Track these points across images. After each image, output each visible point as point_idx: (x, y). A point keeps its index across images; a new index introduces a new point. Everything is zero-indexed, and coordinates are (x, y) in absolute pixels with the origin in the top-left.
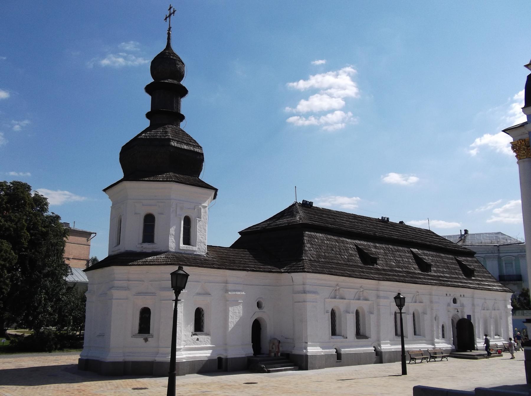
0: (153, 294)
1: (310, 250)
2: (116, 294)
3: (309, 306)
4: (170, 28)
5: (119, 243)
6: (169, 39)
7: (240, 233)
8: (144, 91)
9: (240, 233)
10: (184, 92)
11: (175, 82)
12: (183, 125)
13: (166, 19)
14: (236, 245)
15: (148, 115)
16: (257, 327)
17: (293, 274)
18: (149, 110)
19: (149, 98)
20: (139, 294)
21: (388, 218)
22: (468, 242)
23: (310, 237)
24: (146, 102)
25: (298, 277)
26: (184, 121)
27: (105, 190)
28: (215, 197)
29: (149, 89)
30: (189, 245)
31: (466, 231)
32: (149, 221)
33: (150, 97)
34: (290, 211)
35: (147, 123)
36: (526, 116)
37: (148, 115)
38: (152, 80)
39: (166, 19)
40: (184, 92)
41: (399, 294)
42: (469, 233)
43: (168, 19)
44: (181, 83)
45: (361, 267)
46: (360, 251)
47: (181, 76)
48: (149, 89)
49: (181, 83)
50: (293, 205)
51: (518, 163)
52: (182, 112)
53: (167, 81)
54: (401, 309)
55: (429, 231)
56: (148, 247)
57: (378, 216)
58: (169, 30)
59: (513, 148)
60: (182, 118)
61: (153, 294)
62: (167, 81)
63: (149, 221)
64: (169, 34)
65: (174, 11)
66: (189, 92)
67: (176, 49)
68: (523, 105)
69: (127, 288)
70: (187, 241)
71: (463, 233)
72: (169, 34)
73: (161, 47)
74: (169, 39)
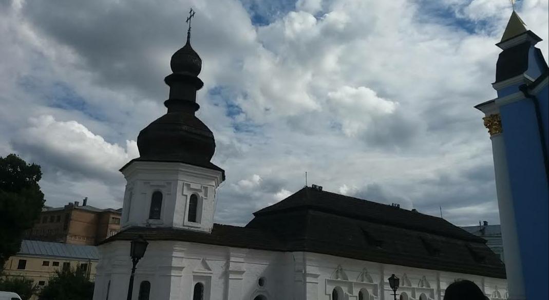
3: (308, 286)
4: (190, 28)
5: (128, 221)
6: (189, 37)
7: (254, 214)
8: (164, 82)
9: (254, 214)
12: (197, 114)
13: (187, 21)
14: (250, 225)
17: (294, 253)
18: (168, 98)
21: (398, 205)
22: (487, 233)
26: (199, 110)
27: (121, 170)
28: (224, 178)
29: (168, 80)
30: (194, 221)
31: (485, 223)
32: (157, 199)
33: (169, 88)
35: (164, 111)
36: (496, 91)
37: (167, 104)
39: (187, 21)
41: (393, 275)
42: (489, 224)
43: (189, 21)
47: (198, 70)
49: (198, 76)
51: (491, 138)
52: (198, 101)
54: (395, 291)
55: (441, 219)
56: (154, 223)
57: (388, 204)
58: (190, 28)
59: (486, 125)
63: (157, 199)
64: (189, 33)
65: (194, 13)
66: (204, 84)
67: (195, 47)
68: (494, 81)
71: (482, 224)
72: (189, 33)
74: (189, 37)
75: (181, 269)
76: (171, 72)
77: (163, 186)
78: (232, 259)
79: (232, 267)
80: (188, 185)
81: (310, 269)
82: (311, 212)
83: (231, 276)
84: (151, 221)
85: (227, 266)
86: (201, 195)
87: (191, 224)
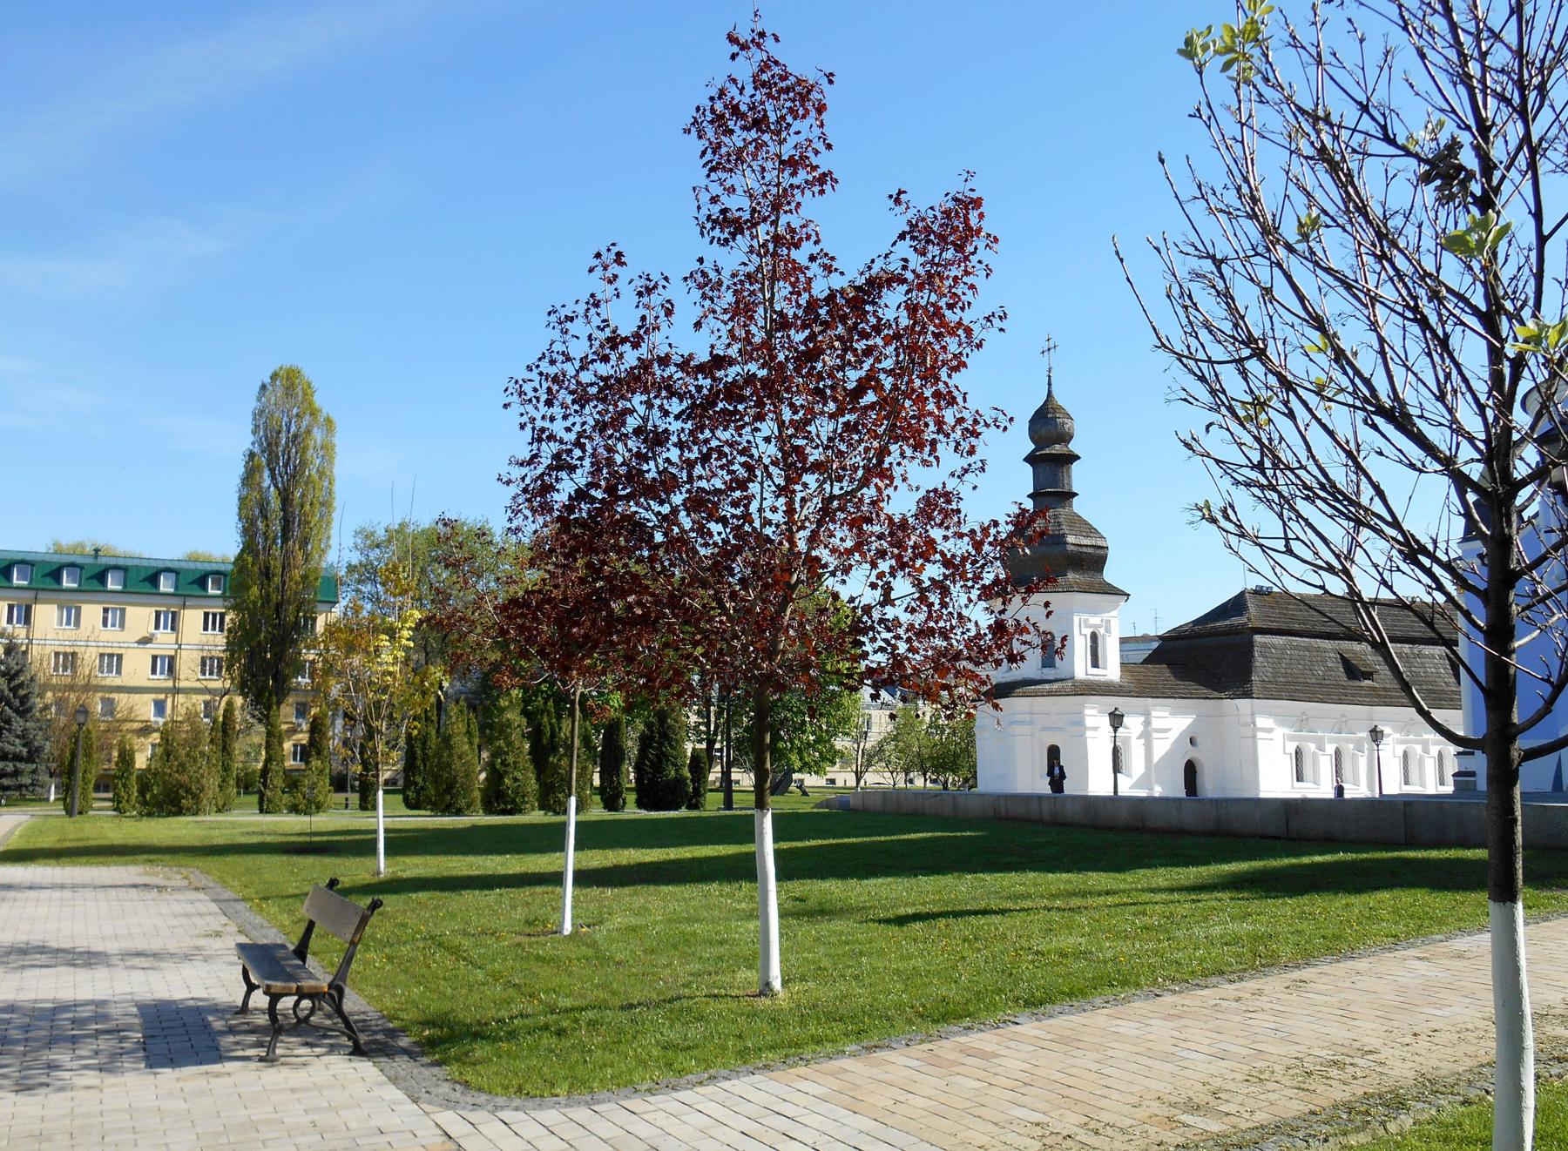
0: (1061, 729)
1: (1262, 667)
2: (1019, 729)
3: (1260, 744)
10: (1074, 458)
12: (1078, 506)
16: (1191, 770)
20: (1044, 729)
23: (1264, 645)
25: (1244, 704)
29: (1030, 459)
34: (1236, 605)
40: (1074, 458)
45: (1344, 687)
46: (1346, 663)
48: (1030, 459)
50: (1243, 593)
52: (1074, 490)
56: (1049, 673)
61: (1061, 729)
67: (1060, 398)
69: (1031, 723)
70: (1095, 664)
75: (1095, 729)
78: (1154, 714)
79: (1156, 724)
80: (1086, 621)
81: (1262, 722)
82: (1258, 638)
83: (1155, 735)
84: (1046, 670)
85: (1147, 723)
86: (1102, 630)
87: (1095, 671)
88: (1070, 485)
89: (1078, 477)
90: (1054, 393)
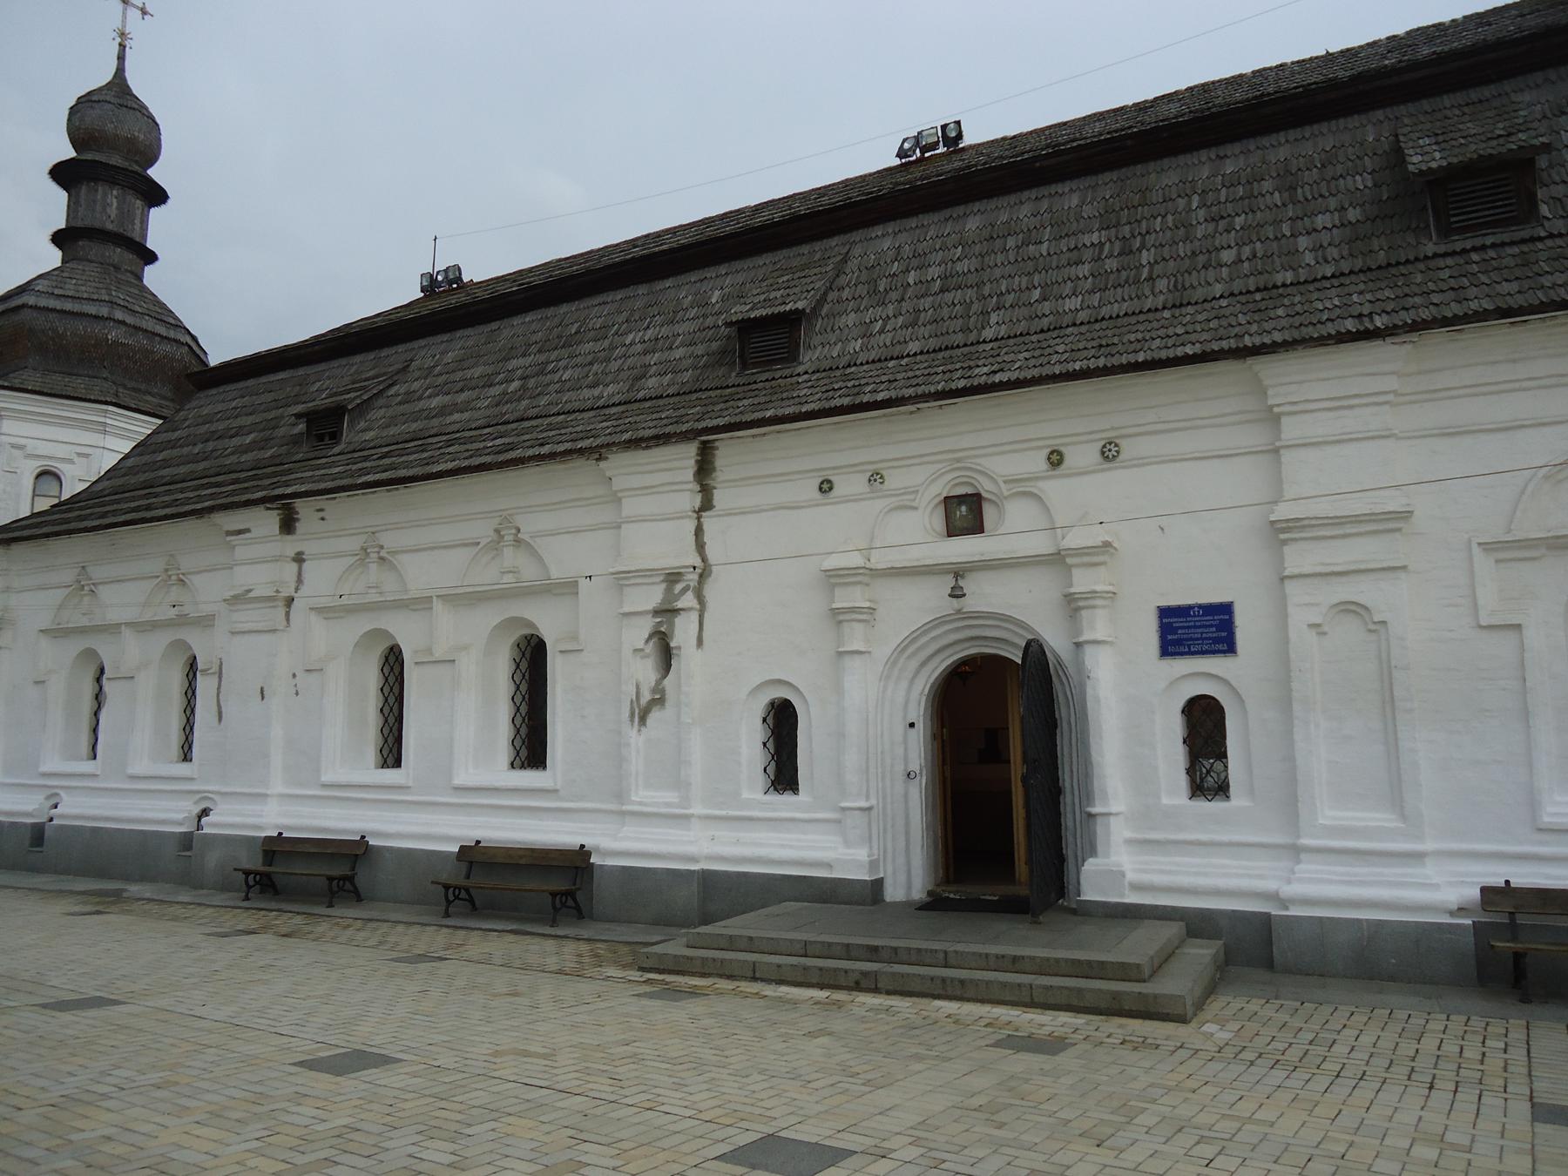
6: (121, 58)
11: (136, 168)
15: (58, 239)
19: (63, 196)
24: (55, 206)
29: (62, 174)
35: (53, 258)
37: (58, 239)
38: (71, 153)
44: (150, 172)
47: (151, 153)
48: (62, 174)
49: (150, 172)
53: (110, 160)
60: (151, 258)
62: (110, 160)
64: (122, 47)
66: (169, 202)
67: (139, 85)
72: (122, 47)
73: (104, 76)
74: (121, 58)
76: (68, 152)
77: (71, 461)
88: (145, 236)
89: (160, 228)
90: (128, 75)
